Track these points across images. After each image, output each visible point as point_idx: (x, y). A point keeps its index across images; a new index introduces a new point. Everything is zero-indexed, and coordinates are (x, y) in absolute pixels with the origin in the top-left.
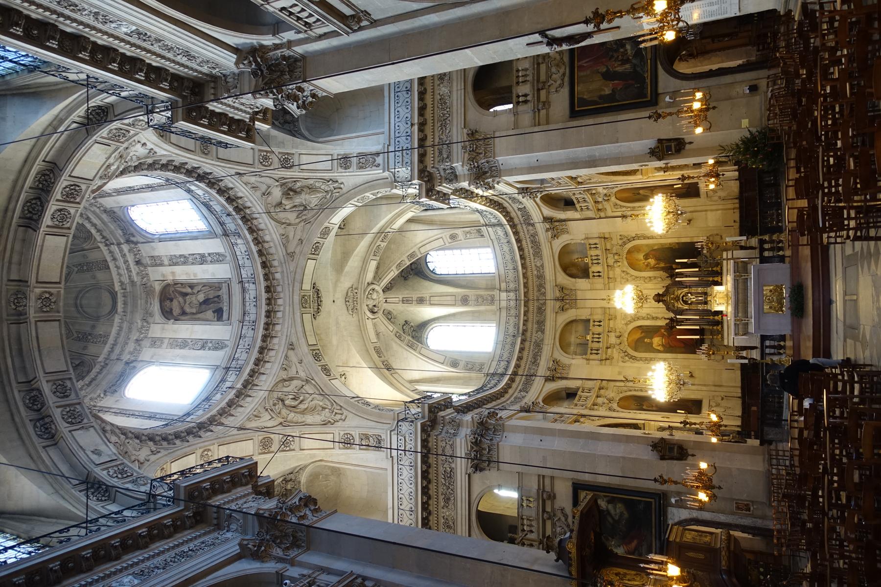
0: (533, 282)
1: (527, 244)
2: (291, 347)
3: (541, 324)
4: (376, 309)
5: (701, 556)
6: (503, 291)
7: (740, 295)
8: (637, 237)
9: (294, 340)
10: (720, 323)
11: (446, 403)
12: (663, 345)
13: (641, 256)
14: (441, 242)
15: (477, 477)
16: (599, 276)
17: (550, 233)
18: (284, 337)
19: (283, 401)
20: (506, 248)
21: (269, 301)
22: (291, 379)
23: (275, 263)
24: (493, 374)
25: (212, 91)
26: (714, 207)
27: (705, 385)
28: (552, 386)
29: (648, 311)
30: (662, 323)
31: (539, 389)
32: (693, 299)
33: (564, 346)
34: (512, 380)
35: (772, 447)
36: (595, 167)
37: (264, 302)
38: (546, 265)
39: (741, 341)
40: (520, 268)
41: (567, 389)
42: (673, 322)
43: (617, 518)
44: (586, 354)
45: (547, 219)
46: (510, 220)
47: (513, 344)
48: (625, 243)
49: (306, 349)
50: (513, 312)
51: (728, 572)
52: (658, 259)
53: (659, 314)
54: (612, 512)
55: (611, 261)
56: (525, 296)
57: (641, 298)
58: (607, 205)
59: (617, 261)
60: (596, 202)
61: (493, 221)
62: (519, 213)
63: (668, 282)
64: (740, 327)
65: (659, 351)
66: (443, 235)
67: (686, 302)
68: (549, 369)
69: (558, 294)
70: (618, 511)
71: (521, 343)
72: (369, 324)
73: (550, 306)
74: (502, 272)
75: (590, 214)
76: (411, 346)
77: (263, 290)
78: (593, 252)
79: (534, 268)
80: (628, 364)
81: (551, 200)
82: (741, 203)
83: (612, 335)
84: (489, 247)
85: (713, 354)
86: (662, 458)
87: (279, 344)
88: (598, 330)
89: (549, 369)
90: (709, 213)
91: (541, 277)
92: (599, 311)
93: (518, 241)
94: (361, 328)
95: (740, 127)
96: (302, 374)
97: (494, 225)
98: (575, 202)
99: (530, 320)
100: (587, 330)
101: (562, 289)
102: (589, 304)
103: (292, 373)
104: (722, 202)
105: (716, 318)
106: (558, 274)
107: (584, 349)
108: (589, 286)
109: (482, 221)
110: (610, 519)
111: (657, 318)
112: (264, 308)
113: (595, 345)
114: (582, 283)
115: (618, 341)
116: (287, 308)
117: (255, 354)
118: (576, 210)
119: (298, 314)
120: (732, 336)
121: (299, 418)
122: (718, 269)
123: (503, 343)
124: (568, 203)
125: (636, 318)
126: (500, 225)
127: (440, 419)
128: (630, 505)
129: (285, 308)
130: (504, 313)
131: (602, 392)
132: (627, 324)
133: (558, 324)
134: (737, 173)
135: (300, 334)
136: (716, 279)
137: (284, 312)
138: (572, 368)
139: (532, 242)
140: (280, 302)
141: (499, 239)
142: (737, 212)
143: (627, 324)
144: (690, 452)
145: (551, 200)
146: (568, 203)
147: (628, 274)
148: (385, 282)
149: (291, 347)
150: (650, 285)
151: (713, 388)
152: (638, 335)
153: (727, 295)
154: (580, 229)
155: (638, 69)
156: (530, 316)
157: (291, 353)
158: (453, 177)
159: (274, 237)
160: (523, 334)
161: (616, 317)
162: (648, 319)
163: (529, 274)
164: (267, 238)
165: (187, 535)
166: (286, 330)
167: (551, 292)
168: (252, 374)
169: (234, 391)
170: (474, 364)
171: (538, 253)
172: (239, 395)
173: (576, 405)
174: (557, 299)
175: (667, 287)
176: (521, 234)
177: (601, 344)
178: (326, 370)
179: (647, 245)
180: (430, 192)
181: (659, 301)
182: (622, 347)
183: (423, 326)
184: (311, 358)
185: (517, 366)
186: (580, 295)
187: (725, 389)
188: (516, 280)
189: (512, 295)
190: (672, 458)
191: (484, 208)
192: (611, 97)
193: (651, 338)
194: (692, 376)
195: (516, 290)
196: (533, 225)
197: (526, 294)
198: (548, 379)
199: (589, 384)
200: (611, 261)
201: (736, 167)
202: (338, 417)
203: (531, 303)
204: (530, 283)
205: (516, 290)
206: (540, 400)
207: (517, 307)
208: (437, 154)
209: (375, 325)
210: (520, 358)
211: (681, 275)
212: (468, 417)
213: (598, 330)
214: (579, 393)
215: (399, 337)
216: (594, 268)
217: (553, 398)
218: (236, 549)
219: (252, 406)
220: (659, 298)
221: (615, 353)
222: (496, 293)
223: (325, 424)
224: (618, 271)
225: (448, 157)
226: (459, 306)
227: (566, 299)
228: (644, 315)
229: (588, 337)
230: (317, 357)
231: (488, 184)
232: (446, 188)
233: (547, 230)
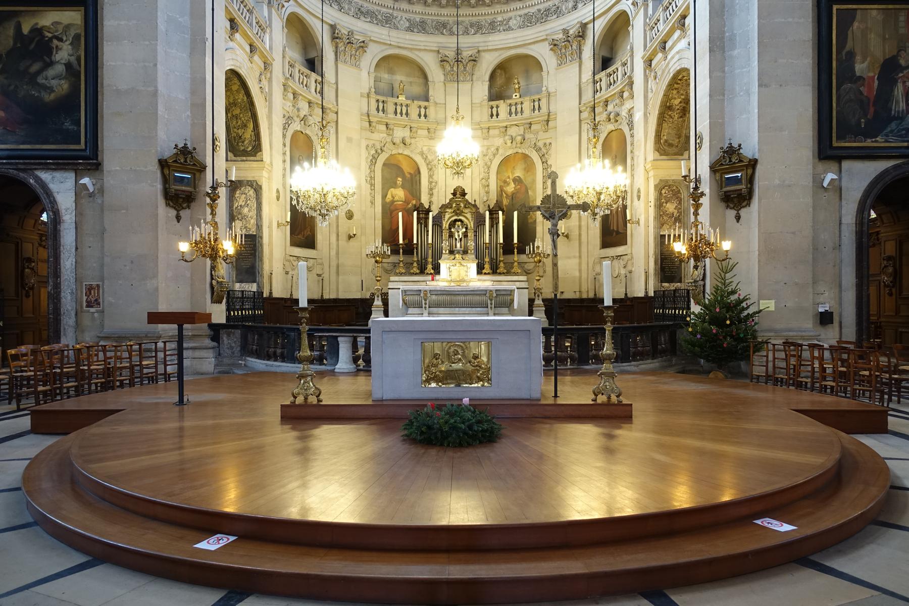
7: (462, 298)
10: (422, 271)
12: (393, 202)
13: (519, 173)
16: (492, 116)
17: (561, 36)
26: (584, 267)
27: (337, 253)
29: (441, 183)
30: (425, 200)
32: (459, 233)
35: (208, 342)
36: (711, 50)
39: (396, 299)
42: (424, 213)
43: (40, 80)
48: (538, 150)
52: (513, 196)
53: (437, 191)
54: (51, 72)
57: (459, 167)
59: (512, 139)
64: (416, 298)
65: (384, 196)
67: (453, 224)
70: (54, 83)
78: (527, 106)
79: (506, 16)
82: (588, 300)
83: (406, 133)
85: (376, 262)
88: (414, 112)
90: (577, 261)
91: (493, 27)
95: (761, 297)
98: (609, 70)
101: (474, 60)
102: (452, 101)
104: (591, 277)
105: (430, 266)
106: (496, 54)
107: (384, 93)
108: (476, 100)
110: (35, 67)
113: (390, 108)
114: (482, 89)
115: (397, 141)
120: (402, 287)
122: (501, 270)
128: (68, 105)
132: (422, 154)
133: (421, 54)
134: (641, 294)
136: (487, 266)
138: (354, 70)
142: (577, 296)
143: (422, 154)
144: (184, 213)
147: (494, 155)
150: (477, 186)
151: (334, 264)
152: (407, 168)
153: (463, 281)
154: (566, 84)
155: (893, 125)
161: (431, 138)
162: (430, 183)
167: (469, 42)
173: (291, 66)
175: (475, 206)
177: (392, 116)
182: (389, 146)
186: (465, 87)
187: (333, 278)
190: (165, 180)
192: (848, 74)
193: (403, 187)
194: (350, 237)
196: (575, 7)
199: (329, 92)
200: (513, 131)
201: (651, 294)
213: (414, 112)
216: (503, 107)
220: (460, 193)
221: (380, 135)
224: (499, 142)
227: (459, 66)
228: (435, 177)
229: (402, 98)
233: (565, 31)
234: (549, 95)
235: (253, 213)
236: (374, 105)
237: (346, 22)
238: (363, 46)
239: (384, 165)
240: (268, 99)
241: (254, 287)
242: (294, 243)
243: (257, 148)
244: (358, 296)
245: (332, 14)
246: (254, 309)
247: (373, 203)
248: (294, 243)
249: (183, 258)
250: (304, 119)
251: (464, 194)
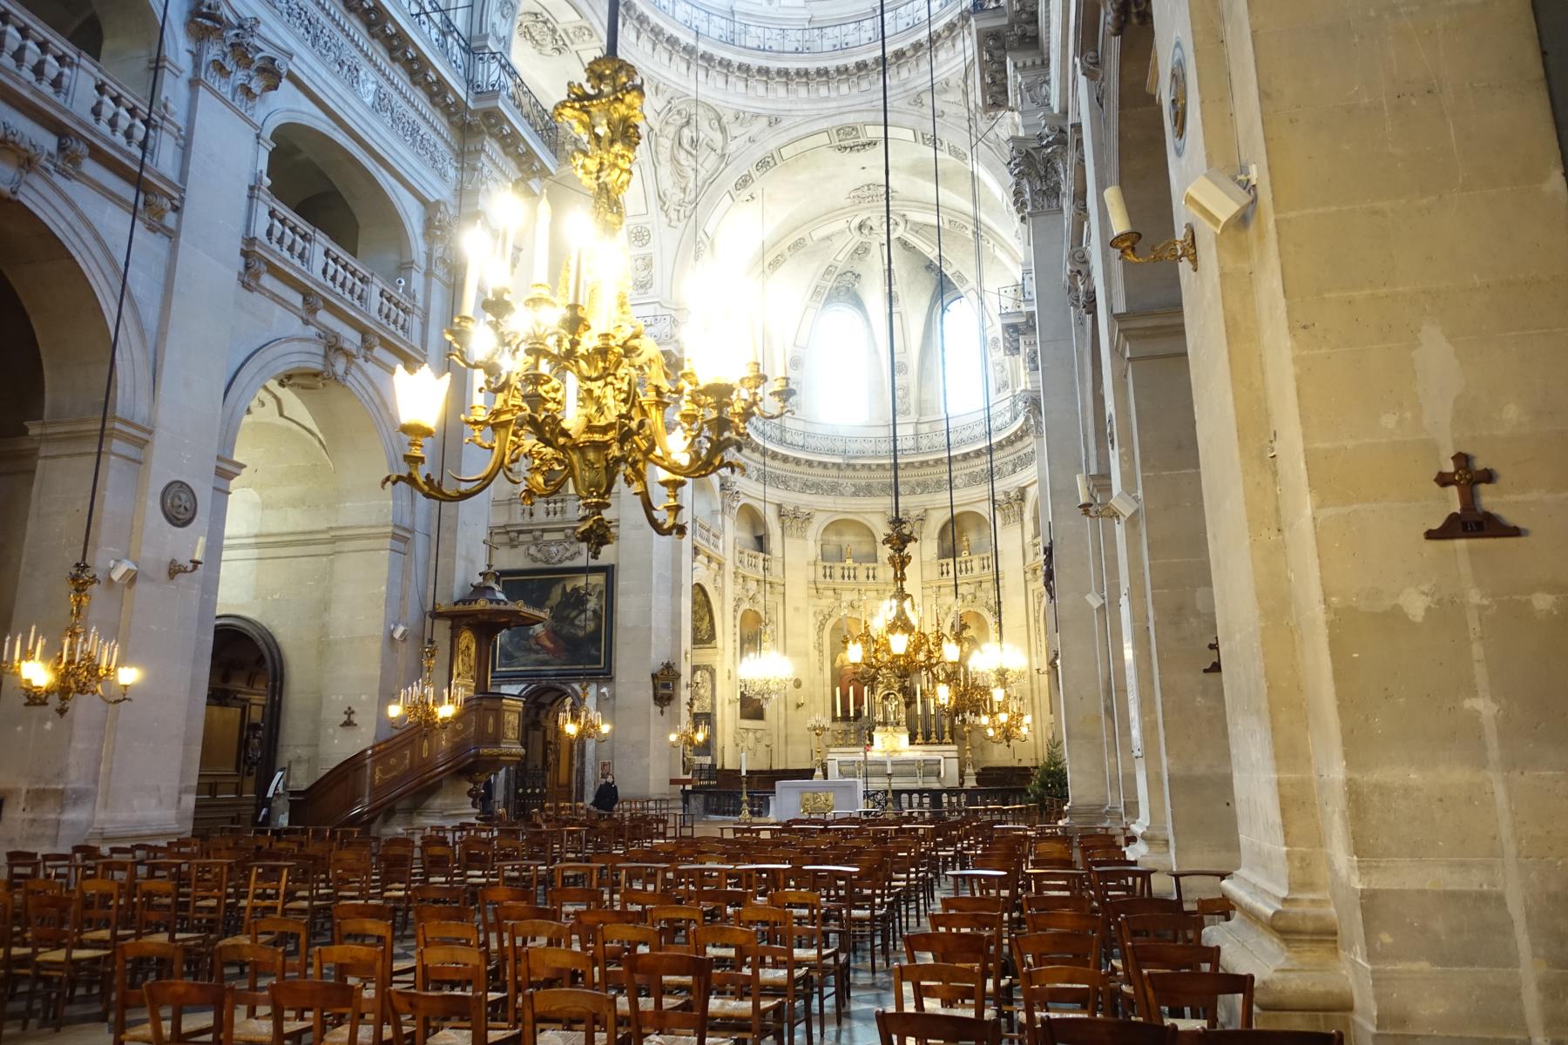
2: (774, 121)
4: (866, 231)
5: (490, 730)
6: (916, 429)
9: (785, 123)
12: (842, 667)
18: (788, 106)
19: (688, 123)
21: (843, 71)
22: (723, 130)
23: (904, 73)
25: (1029, 63)
33: (837, 526)
37: (840, 62)
47: (832, 452)
49: (772, 145)
65: (833, 662)
68: (797, 508)
71: (834, 464)
72: (840, 225)
76: (816, 292)
77: (859, 59)
80: (812, 620)
83: (855, 596)
86: (654, 676)
87: (778, 98)
89: (797, 508)
94: (832, 213)
96: (732, 147)
99: (873, 474)
103: (734, 130)
107: (830, 556)
110: (574, 614)
112: (831, 64)
113: (838, 573)
116: (835, 104)
117: (755, 61)
119: (825, 125)
120: (839, 758)
121: (665, 155)
122: (934, 740)
128: (594, 638)
129: (835, 99)
135: (794, 133)
137: (827, 99)
138: (801, 542)
140: (844, 89)
148: (913, 240)
149: (774, 121)
151: (782, 734)
157: (764, 122)
159: (945, 68)
164: (942, 55)
165: (441, 122)
166: (799, 107)
168: (726, 64)
169: (692, 42)
172: (690, 51)
178: (745, 182)
183: (858, 302)
184: (759, 156)
187: (782, 748)
190: (655, 688)
194: (798, 706)
199: (776, 567)
202: (673, 215)
205: (918, 449)
206: (744, 500)
209: (842, 232)
210: (810, 463)
214: (762, 555)
215: (828, 272)
218: (433, 196)
219: (673, 78)
223: (660, 197)
229: (849, 562)
230: (763, 164)
235: (709, 694)
236: (820, 571)
237: (791, 499)
238: (808, 518)
240: (721, 591)
241: (708, 760)
242: (744, 716)
243: (712, 637)
245: (776, 494)
246: (709, 779)
247: (821, 669)
248: (744, 716)
249: (673, 746)
250: (752, 598)
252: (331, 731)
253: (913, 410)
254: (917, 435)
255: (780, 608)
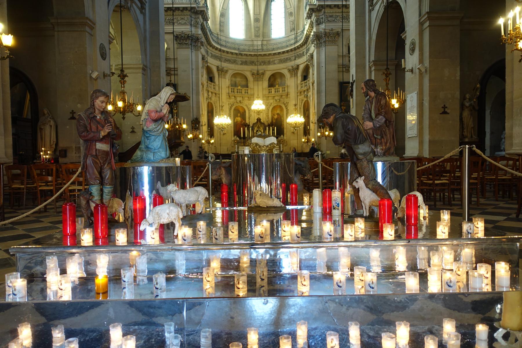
0: (266, 59)
1: (286, 56)
3: (245, 63)
5: (178, 135)
6: (262, 43)
8: (287, 110)
11: (206, 19)
13: (278, 112)
14: (289, 7)
15: (171, 36)
20: (284, 44)
24: (218, 38)
28: (215, 70)
30: (247, 121)
31: (213, 63)
33: (235, 75)
34: (217, 49)
38: (275, 66)
40: (274, 52)
41: (214, 77)
42: (248, 126)
44: (231, 86)
45: (298, 66)
46: (298, 48)
48: (285, 104)
50: (251, 48)
51: (175, 142)
52: (277, 119)
53: (251, 120)
55: (276, 98)
56: (259, 55)
57: (259, 112)
58: (303, 96)
59: (276, 100)
60: (304, 91)
61: (298, 38)
62: (301, 52)
63: (266, 124)
65: (234, 120)
66: (292, 8)
67: (257, 131)
69: (261, 72)
71: (235, 53)
73: (254, 68)
74: (272, 42)
75: (299, 88)
78: (281, 89)
80: (227, 106)
81: (307, 69)
83: (241, 99)
84: (285, 34)
88: (243, 92)
90: (296, 141)
91: (269, 63)
92: (252, 92)
93: (288, 51)
95: (327, 150)
97: (296, 38)
98: (306, 81)
100: (243, 86)
101: (263, 74)
106: (270, 72)
107: (234, 85)
109: (299, 31)
111: (249, 119)
113: (236, 91)
114: (266, 84)
115: (238, 101)
118: (302, 81)
123: (235, 43)
124: (305, 77)
125: (249, 110)
126: (296, 42)
127: (197, 16)
130: (250, 43)
131: (214, 94)
132: (246, 105)
139: (287, 58)
141: (289, 41)
143: (246, 105)
145: (307, 69)
146: (305, 77)
150: (265, 116)
152: (241, 110)
154: (292, 83)
156: (249, 57)
158: (318, 23)
160: (240, 54)
161: (249, 100)
163: (271, 57)
167: (261, 68)
170: (223, 26)
171: (281, 61)
174: (258, 71)
176: (291, 53)
177: (236, 93)
179: (283, 114)
180: (312, 10)
181: (257, 120)
182: (236, 103)
185: (224, 51)
186: (260, 83)
188: (268, 50)
189: (260, 47)
191: (305, 32)
193: (240, 117)
194: (224, 134)
195: (262, 50)
196: (295, 59)
197: (260, 55)
198: (218, 67)
199: (217, 88)
200: (276, 98)
203: (256, 58)
204: (266, 57)
205: (262, 50)
207: (253, 50)
208: (330, 14)
210: (227, 52)
211: (269, 130)
212: (200, 32)
213: (243, 92)
214: (213, 84)
216: (273, 90)
217: (209, 71)
220: (259, 120)
221: (232, 100)
222: (261, 38)
224: (272, 101)
225: (328, 20)
226: (254, 17)
227: (258, 76)
229: (239, 87)
231: (314, 41)
232: (314, 18)
233: (292, 67)
234: (288, 86)
236: (230, 90)
238: (227, 71)
239: (235, 110)
244: (226, 153)
251: (260, 120)
252: (126, 134)
253: (261, 36)
254: (262, 45)
255: (218, 102)
